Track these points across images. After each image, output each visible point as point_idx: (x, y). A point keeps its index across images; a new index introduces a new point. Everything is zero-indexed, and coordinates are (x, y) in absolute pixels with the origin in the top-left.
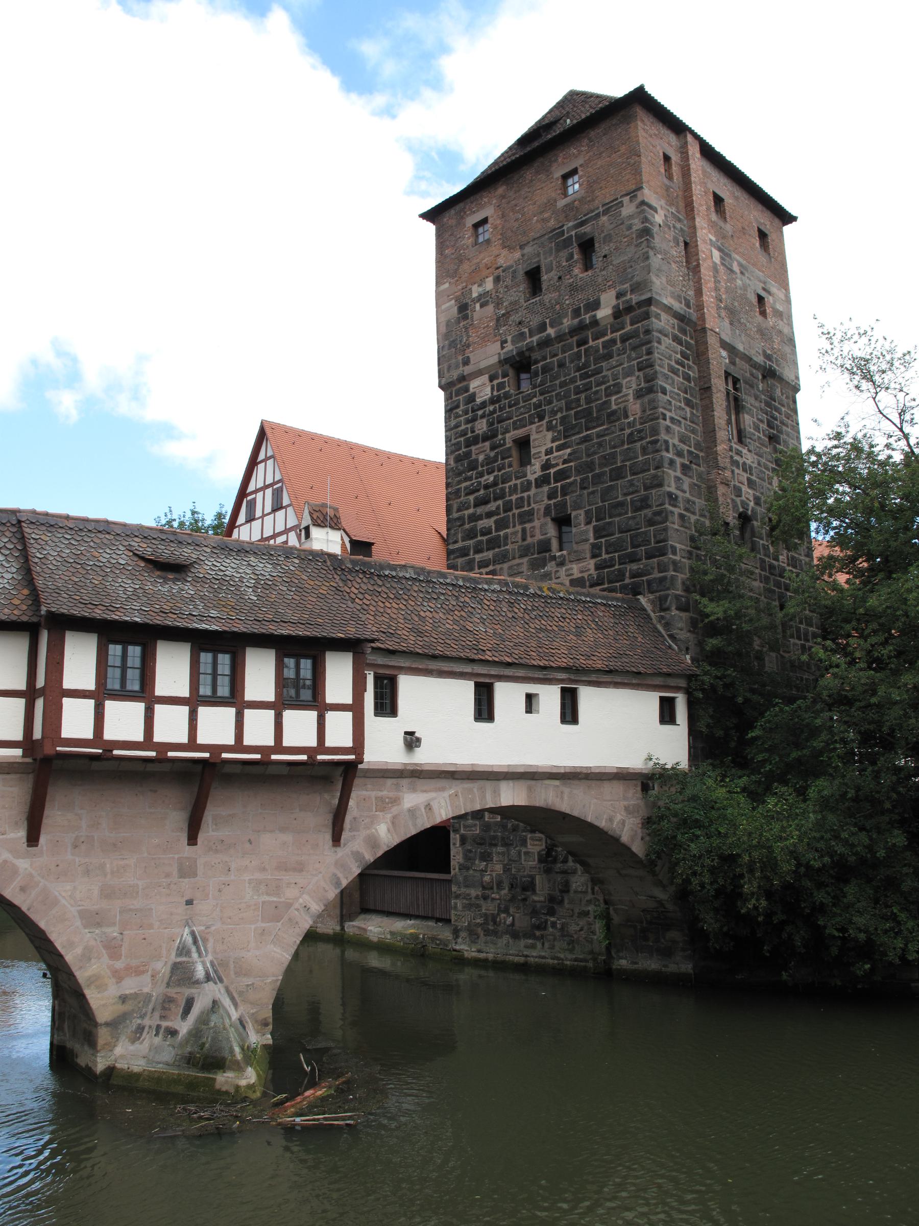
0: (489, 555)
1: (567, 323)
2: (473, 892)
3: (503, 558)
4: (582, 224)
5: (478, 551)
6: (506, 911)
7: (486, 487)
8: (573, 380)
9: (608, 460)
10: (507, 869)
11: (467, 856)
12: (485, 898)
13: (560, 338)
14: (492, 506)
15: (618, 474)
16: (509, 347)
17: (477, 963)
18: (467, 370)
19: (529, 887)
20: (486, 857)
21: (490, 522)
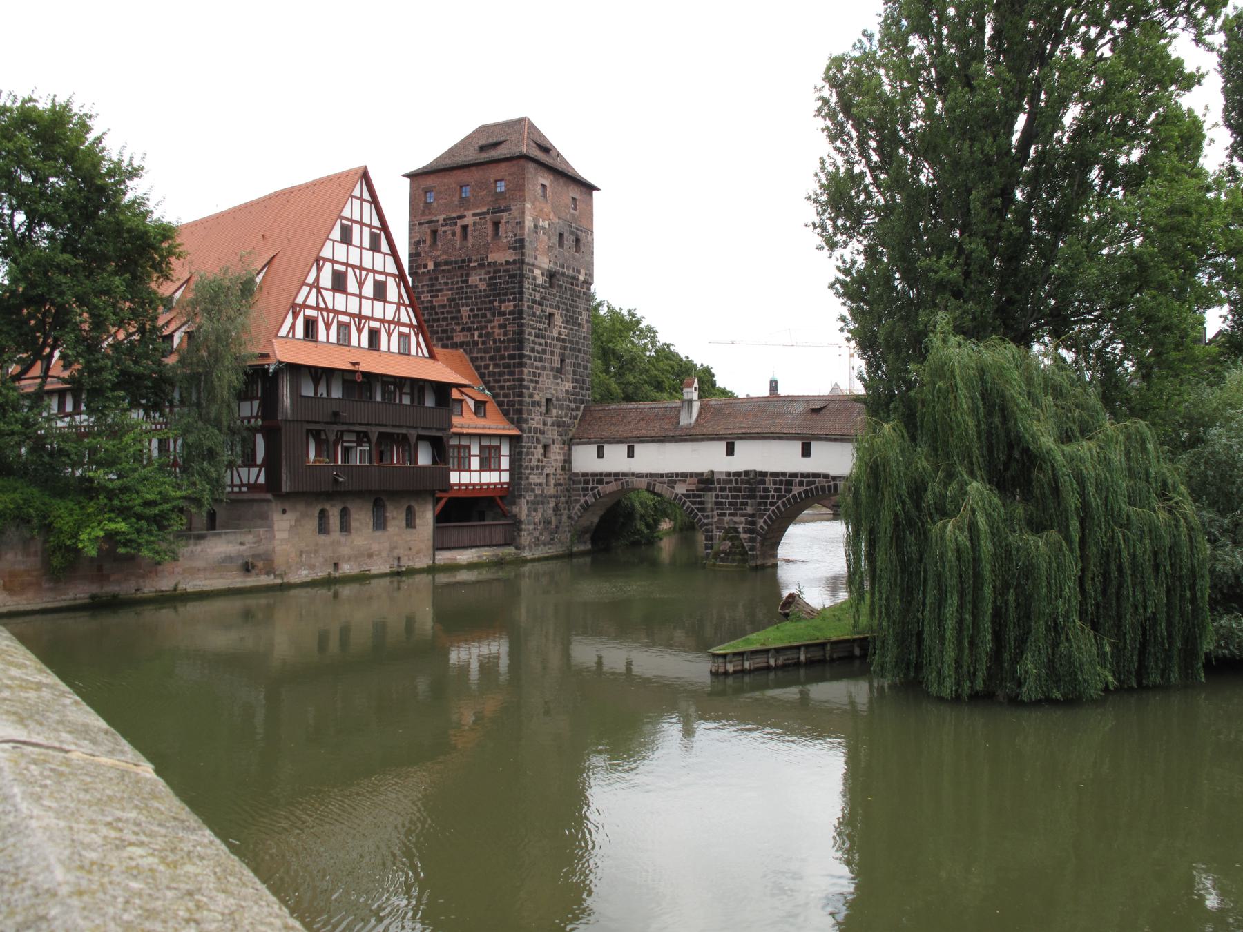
0: (539, 364)
1: (571, 272)
2: (531, 527)
3: (544, 368)
4: (577, 229)
5: (535, 360)
9: (577, 343)
11: (529, 510)
13: (568, 276)
14: (542, 341)
17: (533, 560)
18: (537, 263)
19: (549, 523)
20: (535, 510)
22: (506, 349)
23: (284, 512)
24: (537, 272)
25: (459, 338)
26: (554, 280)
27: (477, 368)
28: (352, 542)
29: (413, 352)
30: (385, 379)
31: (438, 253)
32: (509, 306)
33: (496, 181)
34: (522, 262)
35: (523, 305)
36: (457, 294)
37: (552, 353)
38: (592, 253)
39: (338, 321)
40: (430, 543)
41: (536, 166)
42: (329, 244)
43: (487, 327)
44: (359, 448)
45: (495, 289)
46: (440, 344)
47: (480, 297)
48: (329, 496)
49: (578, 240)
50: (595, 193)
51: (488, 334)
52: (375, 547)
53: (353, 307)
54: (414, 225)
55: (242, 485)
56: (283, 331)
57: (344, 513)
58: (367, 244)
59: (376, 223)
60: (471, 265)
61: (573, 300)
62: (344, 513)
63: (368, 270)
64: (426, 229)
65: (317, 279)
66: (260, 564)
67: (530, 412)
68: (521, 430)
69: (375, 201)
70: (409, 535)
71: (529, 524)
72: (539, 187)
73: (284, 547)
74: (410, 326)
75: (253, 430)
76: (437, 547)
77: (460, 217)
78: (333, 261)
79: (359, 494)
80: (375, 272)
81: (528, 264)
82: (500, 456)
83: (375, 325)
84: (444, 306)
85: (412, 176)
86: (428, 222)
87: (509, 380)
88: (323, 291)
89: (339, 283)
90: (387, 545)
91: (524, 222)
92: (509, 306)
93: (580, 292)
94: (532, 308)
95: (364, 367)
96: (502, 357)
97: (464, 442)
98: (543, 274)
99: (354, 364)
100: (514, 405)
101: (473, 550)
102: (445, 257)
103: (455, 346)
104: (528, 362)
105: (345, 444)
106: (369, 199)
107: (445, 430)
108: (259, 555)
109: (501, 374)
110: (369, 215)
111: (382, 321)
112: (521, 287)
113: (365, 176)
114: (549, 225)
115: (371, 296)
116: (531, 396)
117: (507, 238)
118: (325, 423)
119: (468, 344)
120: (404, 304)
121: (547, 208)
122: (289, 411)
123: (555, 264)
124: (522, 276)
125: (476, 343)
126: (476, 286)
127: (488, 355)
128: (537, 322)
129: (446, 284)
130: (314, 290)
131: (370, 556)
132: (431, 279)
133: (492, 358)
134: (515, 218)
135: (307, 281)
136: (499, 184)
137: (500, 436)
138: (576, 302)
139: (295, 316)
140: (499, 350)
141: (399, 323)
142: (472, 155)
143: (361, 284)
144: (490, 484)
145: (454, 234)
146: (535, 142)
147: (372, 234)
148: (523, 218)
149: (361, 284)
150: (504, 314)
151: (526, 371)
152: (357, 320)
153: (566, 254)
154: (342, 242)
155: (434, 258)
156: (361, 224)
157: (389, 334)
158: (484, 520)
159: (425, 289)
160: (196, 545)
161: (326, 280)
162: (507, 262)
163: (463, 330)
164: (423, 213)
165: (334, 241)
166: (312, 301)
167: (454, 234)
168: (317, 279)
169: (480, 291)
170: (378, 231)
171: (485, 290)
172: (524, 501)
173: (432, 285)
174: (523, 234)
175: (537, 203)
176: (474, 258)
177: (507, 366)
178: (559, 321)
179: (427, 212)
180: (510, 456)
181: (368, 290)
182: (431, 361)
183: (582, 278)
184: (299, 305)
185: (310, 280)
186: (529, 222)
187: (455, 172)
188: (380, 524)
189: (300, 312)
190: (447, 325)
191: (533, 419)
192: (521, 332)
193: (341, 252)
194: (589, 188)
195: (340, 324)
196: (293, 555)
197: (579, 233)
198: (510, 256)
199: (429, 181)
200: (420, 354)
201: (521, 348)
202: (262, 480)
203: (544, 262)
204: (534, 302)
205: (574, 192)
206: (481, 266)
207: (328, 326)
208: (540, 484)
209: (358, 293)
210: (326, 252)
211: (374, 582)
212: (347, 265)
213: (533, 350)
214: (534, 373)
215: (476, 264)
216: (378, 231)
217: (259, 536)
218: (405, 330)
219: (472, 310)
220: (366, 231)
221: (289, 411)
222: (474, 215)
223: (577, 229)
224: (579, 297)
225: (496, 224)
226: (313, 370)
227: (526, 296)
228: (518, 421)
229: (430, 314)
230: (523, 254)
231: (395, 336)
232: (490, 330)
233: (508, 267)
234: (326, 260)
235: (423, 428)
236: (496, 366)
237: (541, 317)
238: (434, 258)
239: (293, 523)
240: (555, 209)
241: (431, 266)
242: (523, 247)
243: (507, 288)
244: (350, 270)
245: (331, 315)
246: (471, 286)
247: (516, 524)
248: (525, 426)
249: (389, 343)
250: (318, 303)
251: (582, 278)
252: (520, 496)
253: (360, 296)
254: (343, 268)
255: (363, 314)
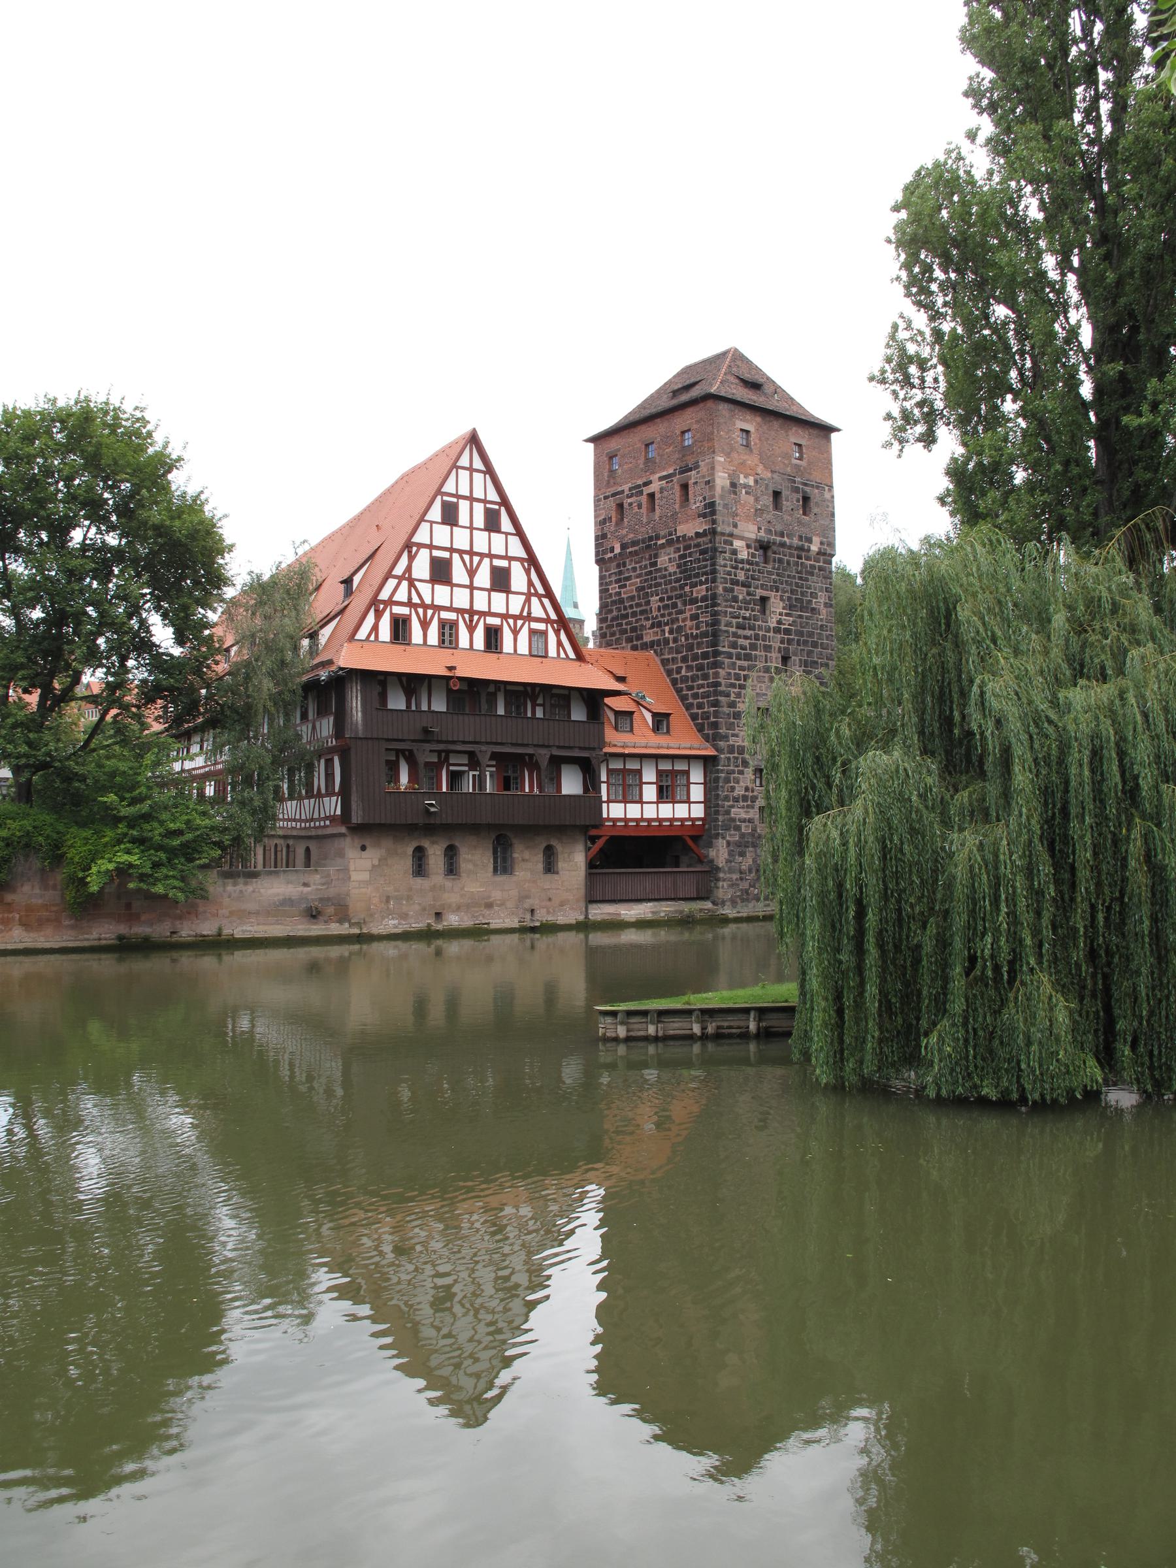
0: (745, 664)
1: (795, 541)
2: (735, 876)
4: (805, 484)
5: (739, 658)
6: (754, 886)
7: (744, 618)
8: (794, 577)
9: (811, 634)
10: (754, 861)
11: (730, 854)
12: (741, 879)
13: (790, 547)
14: (748, 633)
15: (815, 645)
16: (762, 534)
17: (737, 920)
18: (736, 532)
20: (742, 854)
21: (746, 643)
22: (699, 645)
23: (363, 848)
24: (738, 544)
25: (649, 636)
26: (770, 553)
27: (669, 673)
28: (462, 889)
29: (552, 652)
30: (509, 687)
31: (624, 532)
32: (700, 591)
33: (683, 433)
34: (713, 532)
35: (717, 587)
36: (646, 581)
37: (768, 648)
38: (833, 515)
39: (439, 619)
40: (582, 892)
41: (731, 406)
42: (425, 526)
43: (677, 619)
44: (471, 773)
45: (685, 571)
46: (629, 645)
47: (670, 582)
48: (431, 828)
49: (806, 499)
50: (834, 436)
51: (680, 629)
52: (497, 895)
53: (461, 599)
54: (599, 500)
55: (326, 818)
56: (362, 634)
57: (451, 853)
58: (479, 521)
59: (493, 496)
60: (660, 542)
61: (801, 578)
62: (451, 853)
63: (482, 556)
64: (611, 502)
65: (409, 569)
66: (331, 910)
67: (731, 726)
68: (717, 750)
69: (489, 471)
70: (547, 881)
71: (731, 871)
72: (739, 433)
73: (363, 890)
74: (547, 620)
75: (332, 750)
76: (591, 900)
77: (646, 484)
78: (431, 547)
79: (474, 829)
80: (491, 556)
81: (723, 534)
82: (689, 783)
83: (495, 621)
84: (632, 598)
85: (596, 440)
86: (614, 495)
87: (702, 686)
88: (417, 583)
89: (441, 572)
90: (514, 893)
91: (714, 481)
92: (700, 591)
93: (813, 567)
94: (732, 590)
95: (459, 673)
96: (695, 658)
97: (632, 765)
98: (748, 546)
99: (451, 668)
100: (708, 718)
101: (650, 904)
102: (631, 536)
103: (645, 646)
104: (727, 661)
105: (451, 768)
106: (483, 468)
107: (594, 749)
108: (328, 899)
109: (694, 679)
110: (481, 486)
111: (505, 616)
112: (713, 564)
113: (473, 440)
114: (756, 482)
115: (488, 586)
116: (732, 705)
117: (696, 504)
118: (413, 741)
119: (658, 642)
120: (537, 594)
121: (752, 460)
122: (360, 727)
123: (769, 531)
124: (715, 550)
125: (666, 641)
126: (666, 569)
127: (679, 656)
128: (740, 608)
129: (634, 569)
130: (405, 584)
131: (489, 906)
132: (618, 566)
133: (684, 659)
134: (704, 477)
135: (394, 573)
136: (687, 435)
137: (688, 758)
138: (807, 580)
139: (379, 615)
140: (690, 648)
141: (529, 618)
142: (665, 403)
143: (472, 573)
144: (672, 820)
145: (640, 506)
146: (738, 377)
147: (488, 512)
148: (713, 474)
149: (472, 573)
150: (694, 601)
151: (722, 672)
152: (467, 616)
153: (786, 517)
154: (443, 523)
155: (620, 538)
156: (471, 499)
157: (515, 632)
158: (678, 866)
159: (613, 578)
160: (246, 884)
161: (422, 567)
162: (698, 535)
163: (652, 626)
164: (608, 485)
165: (432, 523)
166: (402, 595)
167: (640, 506)
168: (409, 569)
169: (670, 575)
170: (497, 507)
171: (675, 573)
172: (721, 843)
173: (620, 573)
174: (714, 496)
175: (735, 455)
176: (662, 533)
177: (700, 668)
178: (777, 606)
179: (612, 481)
180: (705, 784)
181: (483, 578)
182: (578, 663)
183: (814, 548)
184: (383, 602)
185: (399, 570)
186: (721, 480)
187: (639, 428)
188: (503, 865)
189: (384, 610)
190: (637, 621)
191: (736, 736)
192: (715, 623)
193: (442, 535)
194: (826, 430)
195: (443, 624)
196: (375, 900)
197: (807, 489)
198: (700, 526)
199: (614, 444)
200: (562, 655)
201: (714, 644)
202: (338, 812)
203: (750, 530)
204: (735, 582)
205: (798, 435)
206: (670, 543)
207: (425, 625)
208: (750, 821)
209: (467, 582)
210: (422, 536)
211: (496, 940)
212: (451, 550)
213: (734, 645)
214: (737, 677)
215: (664, 541)
216: (497, 507)
217: (329, 875)
218: (541, 626)
219: (662, 600)
220: (479, 509)
221: (360, 727)
222: (661, 479)
223: (805, 484)
224: (812, 574)
225: (685, 487)
226: (404, 679)
227: (720, 575)
228: (712, 738)
229: (619, 610)
230: (714, 522)
231: (524, 635)
232: (681, 624)
233: (699, 540)
234: (420, 546)
235: (559, 747)
236: (689, 668)
237: (745, 601)
238: (620, 538)
239: (376, 862)
240: (765, 460)
241: (617, 550)
242: (713, 513)
243: (699, 568)
244: (456, 556)
245: (430, 612)
246: (660, 570)
247: (712, 872)
248: (722, 744)
249: (516, 643)
250: (410, 598)
251: (814, 548)
252: (717, 836)
253: (472, 588)
254: (446, 555)
255: (475, 608)
